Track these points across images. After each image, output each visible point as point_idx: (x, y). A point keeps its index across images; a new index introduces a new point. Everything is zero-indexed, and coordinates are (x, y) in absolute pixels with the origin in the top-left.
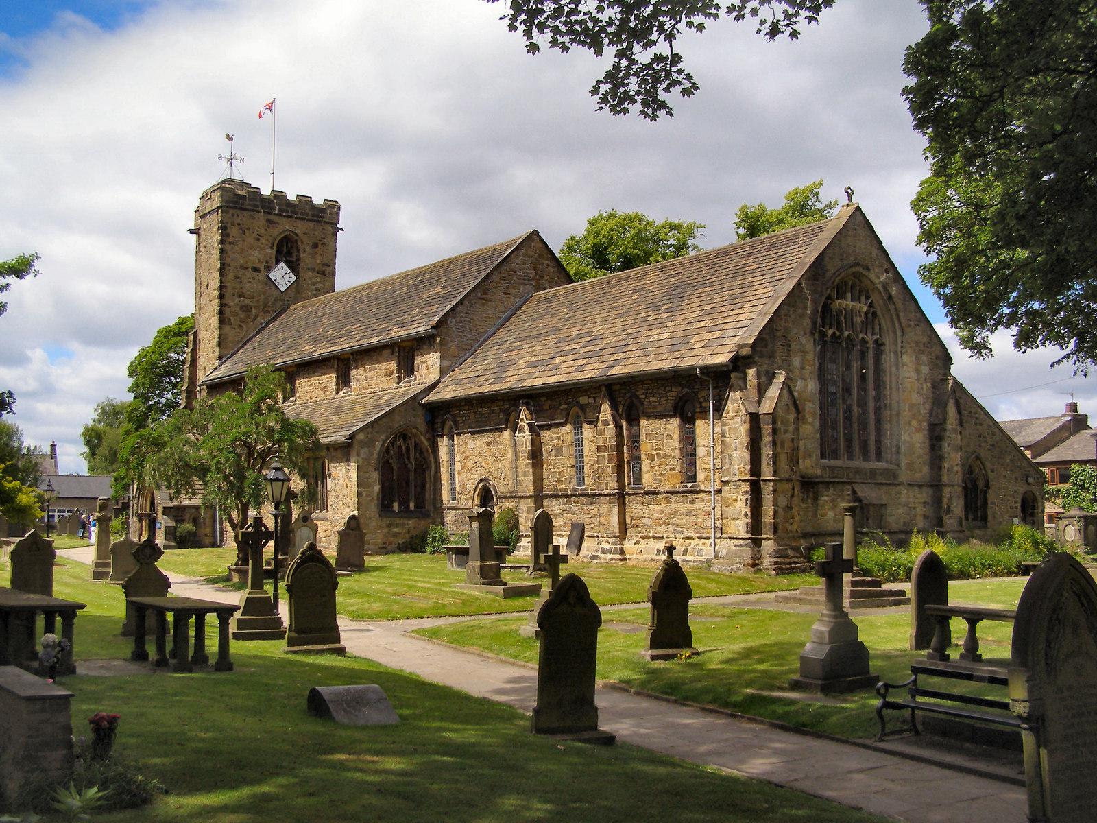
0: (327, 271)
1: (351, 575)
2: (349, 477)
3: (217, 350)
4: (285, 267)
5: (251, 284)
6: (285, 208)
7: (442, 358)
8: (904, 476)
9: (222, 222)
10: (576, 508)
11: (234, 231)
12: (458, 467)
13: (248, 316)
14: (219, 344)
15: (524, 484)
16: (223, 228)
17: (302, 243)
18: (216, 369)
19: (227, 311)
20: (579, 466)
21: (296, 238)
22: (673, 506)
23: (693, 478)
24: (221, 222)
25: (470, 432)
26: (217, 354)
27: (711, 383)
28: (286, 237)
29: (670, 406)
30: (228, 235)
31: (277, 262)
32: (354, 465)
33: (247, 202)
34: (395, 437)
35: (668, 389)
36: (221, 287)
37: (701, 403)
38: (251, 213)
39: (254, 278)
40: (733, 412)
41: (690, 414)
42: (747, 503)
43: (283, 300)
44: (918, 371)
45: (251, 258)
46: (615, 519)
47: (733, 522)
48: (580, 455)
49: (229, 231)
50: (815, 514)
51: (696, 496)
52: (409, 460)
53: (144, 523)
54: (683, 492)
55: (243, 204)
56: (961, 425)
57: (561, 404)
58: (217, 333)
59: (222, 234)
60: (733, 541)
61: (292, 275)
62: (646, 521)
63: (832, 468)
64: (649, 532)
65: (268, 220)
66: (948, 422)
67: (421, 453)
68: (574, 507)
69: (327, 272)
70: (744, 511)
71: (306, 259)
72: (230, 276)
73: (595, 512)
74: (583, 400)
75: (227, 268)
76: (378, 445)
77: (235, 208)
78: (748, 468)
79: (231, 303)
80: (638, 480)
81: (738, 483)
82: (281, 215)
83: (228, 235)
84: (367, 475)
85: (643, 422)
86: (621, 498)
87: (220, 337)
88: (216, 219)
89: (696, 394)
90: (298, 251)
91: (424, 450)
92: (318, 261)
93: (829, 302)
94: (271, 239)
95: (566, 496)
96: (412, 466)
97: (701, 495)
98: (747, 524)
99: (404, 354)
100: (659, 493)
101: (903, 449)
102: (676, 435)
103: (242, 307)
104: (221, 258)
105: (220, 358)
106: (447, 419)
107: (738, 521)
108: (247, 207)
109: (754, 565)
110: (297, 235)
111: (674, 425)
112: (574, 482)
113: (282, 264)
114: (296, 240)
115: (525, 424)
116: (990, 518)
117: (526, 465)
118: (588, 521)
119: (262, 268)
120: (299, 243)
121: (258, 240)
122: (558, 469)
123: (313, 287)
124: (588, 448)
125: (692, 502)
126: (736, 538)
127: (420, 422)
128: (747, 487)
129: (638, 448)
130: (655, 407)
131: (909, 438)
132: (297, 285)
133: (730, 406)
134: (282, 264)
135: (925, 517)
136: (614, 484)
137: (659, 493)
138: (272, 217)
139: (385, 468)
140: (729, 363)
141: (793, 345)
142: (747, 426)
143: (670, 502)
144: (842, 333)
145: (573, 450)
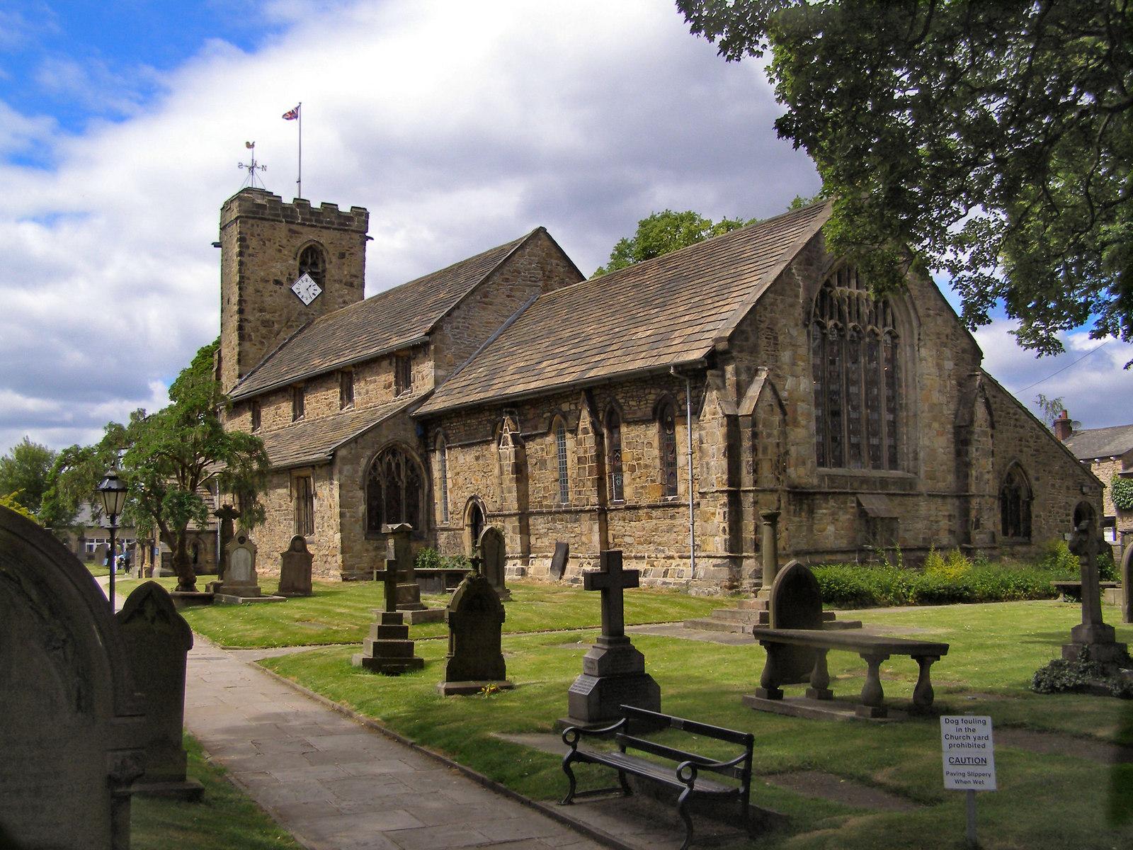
0: (356, 281)
1: (285, 601)
2: (332, 496)
3: (237, 367)
4: (309, 279)
6: (308, 217)
7: (437, 367)
8: (923, 486)
9: (240, 233)
10: (561, 527)
11: (253, 243)
12: (450, 484)
13: (270, 332)
14: (239, 361)
15: (509, 501)
18: (235, 388)
19: (247, 327)
20: (563, 480)
21: (321, 248)
22: (654, 522)
23: (674, 491)
24: (240, 233)
25: (460, 446)
26: (237, 373)
27: (687, 383)
28: (310, 247)
29: (649, 410)
31: (301, 273)
32: (336, 482)
33: (267, 211)
34: (383, 452)
35: (647, 391)
36: (241, 301)
37: (680, 406)
38: (272, 223)
39: (275, 292)
40: (710, 414)
41: (670, 419)
42: (725, 518)
43: (307, 314)
44: (939, 367)
46: (596, 538)
47: (711, 538)
48: (563, 468)
49: (248, 242)
50: (810, 529)
51: (676, 510)
52: (399, 475)
53: (146, 550)
54: (663, 506)
56: (992, 426)
57: (544, 413)
58: (237, 349)
59: (240, 246)
60: (711, 560)
61: (317, 287)
62: (628, 539)
63: (832, 478)
64: (631, 552)
65: (290, 230)
66: (976, 424)
67: (413, 469)
68: (559, 525)
69: (355, 283)
70: (722, 525)
72: (250, 290)
73: (578, 530)
74: (565, 407)
75: (246, 281)
76: (363, 462)
77: (254, 218)
78: (725, 477)
79: (251, 318)
80: (620, 494)
81: (716, 495)
82: (304, 224)
83: (248, 247)
84: (350, 494)
85: (624, 429)
86: (602, 513)
87: (239, 355)
88: (235, 230)
89: (675, 396)
90: (324, 262)
91: (416, 466)
92: (346, 273)
93: (829, 289)
95: (550, 513)
96: (403, 483)
97: (682, 509)
98: (725, 540)
99: (401, 362)
100: (639, 508)
101: (921, 455)
102: (656, 443)
104: (240, 271)
105: (240, 376)
106: (439, 432)
107: (717, 538)
108: (267, 217)
109: (731, 587)
110: (322, 245)
111: (653, 431)
112: (558, 497)
113: (306, 276)
115: (508, 435)
116: (1034, 533)
117: (511, 480)
118: (573, 541)
119: (284, 280)
120: (325, 253)
121: (280, 251)
122: (543, 483)
123: (341, 300)
124: (571, 459)
125: (673, 517)
126: (715, 557)
127: (410, 436)
128: (724, 499)
129: (619, 459)
130: (635, 412)
131: (929, 442)
132: (323, 298)
133: (707, 408)
134: (306, 276)
135: (951, 532)
136: (594, 499)
137: (639, 508)
138: (294, 227)
139: (372, 488)
140: (703, 359)
141: (781, 338)
142: (724, 430)
143: (651, 518)
144: (845, 324)
145: (556, 463)
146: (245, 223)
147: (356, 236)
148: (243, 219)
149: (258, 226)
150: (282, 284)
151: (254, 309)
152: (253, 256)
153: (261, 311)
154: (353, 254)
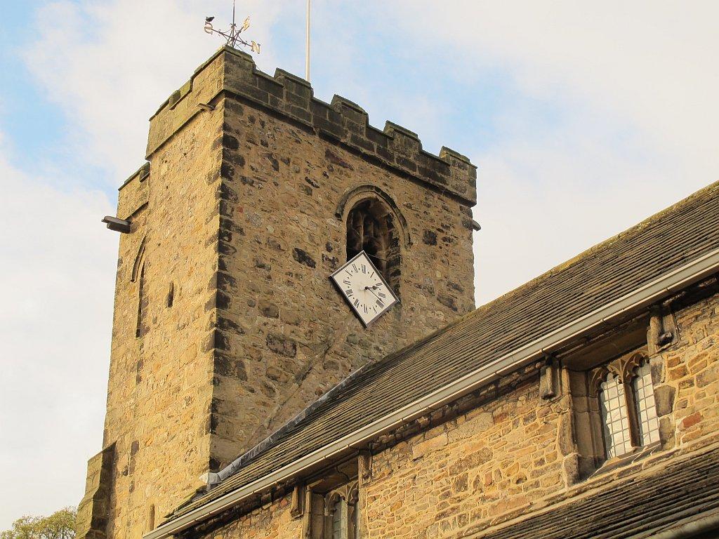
3: (207, 439)
5: (296, 293)
9: (225, 127)
11: (253, 156)
14: (213, 425)
16: (228, 142)
17: (405, 224)
21: (390, 211)
26: (203, 456)
30: (241, 162)
31: (351, 254)
36: (222, 278)
38: (295, 129)
45: (293, 227)
49: (242, 152)
55: (275, 102)
61: (383, 289)
69: (458, 303)
71: (412, 257)
72: (243, 257)
75: (236, 236)
79: (243, 322)
87: (214, 406)
92: (439, 275)
94: (336, 198)
103: (270, 340)
104: (222, 209)
105: (214, 465)
108: (284, 112)
110: (393, 204)
113: (362, 260)
114: (389, 217)
119: (317, 257)
120: (396, 223)
132: (398, 315)
134: (362, 260)
146: (238, 111)
147: (455, 206)
148: (231, 101)
149: (263, 124)
150: (312, 264)
151: (251, 305)
152: (251, 184)
153: (267, 312)
154: (450, 240)
